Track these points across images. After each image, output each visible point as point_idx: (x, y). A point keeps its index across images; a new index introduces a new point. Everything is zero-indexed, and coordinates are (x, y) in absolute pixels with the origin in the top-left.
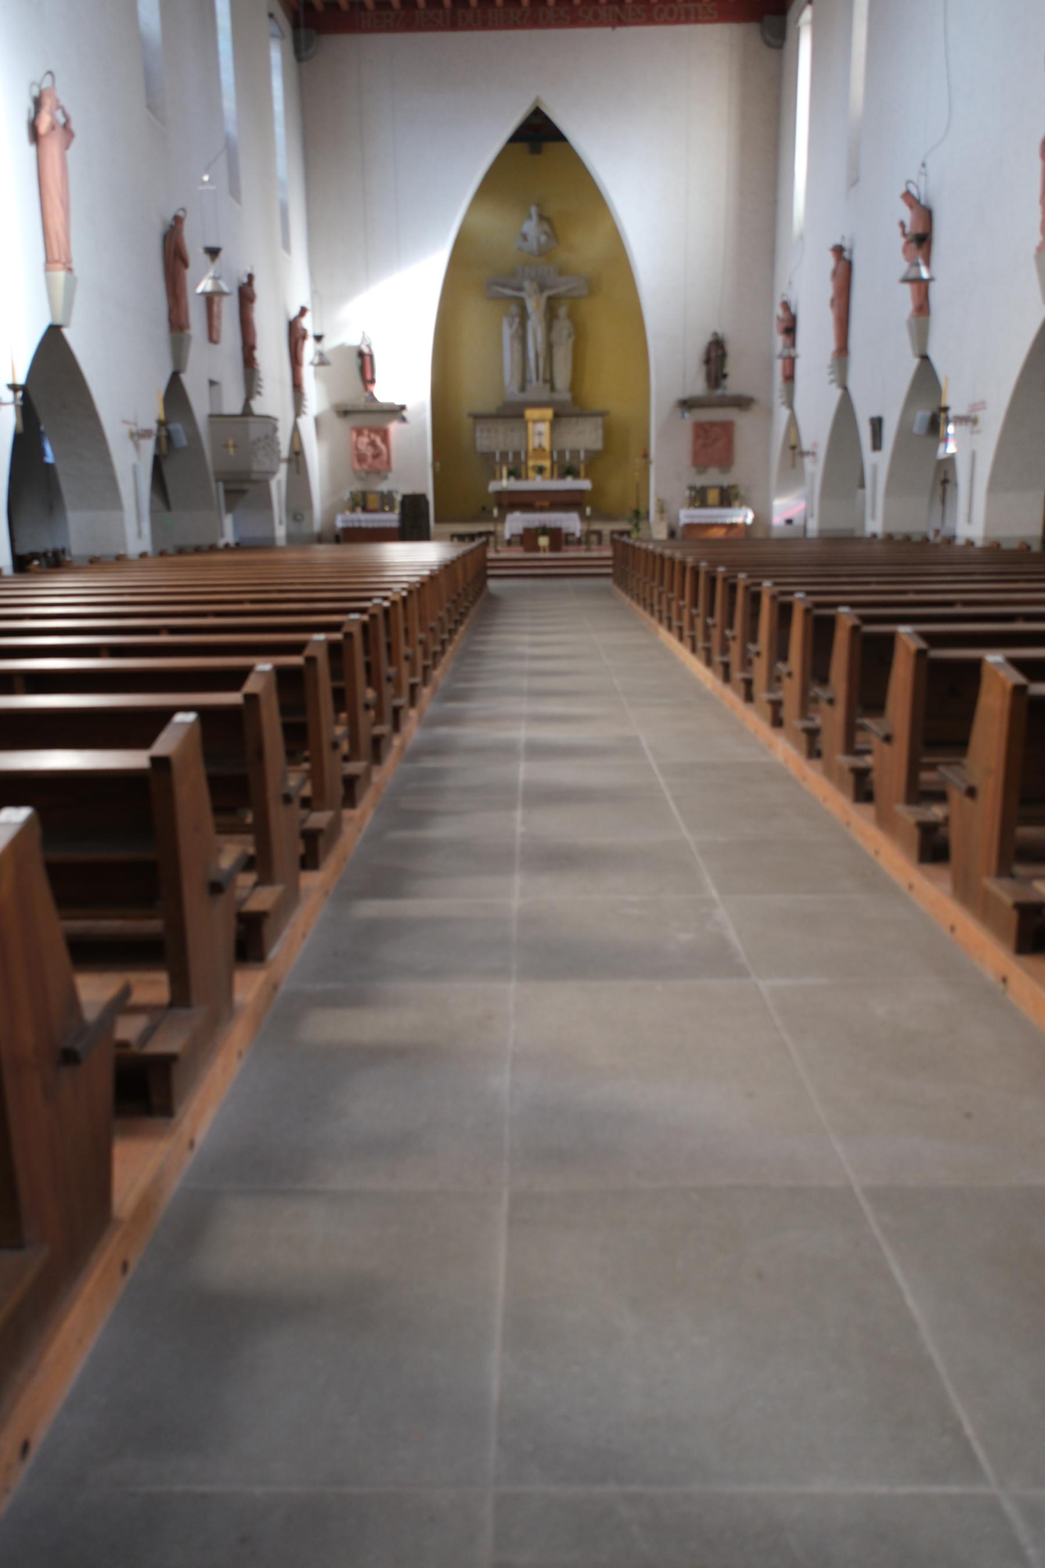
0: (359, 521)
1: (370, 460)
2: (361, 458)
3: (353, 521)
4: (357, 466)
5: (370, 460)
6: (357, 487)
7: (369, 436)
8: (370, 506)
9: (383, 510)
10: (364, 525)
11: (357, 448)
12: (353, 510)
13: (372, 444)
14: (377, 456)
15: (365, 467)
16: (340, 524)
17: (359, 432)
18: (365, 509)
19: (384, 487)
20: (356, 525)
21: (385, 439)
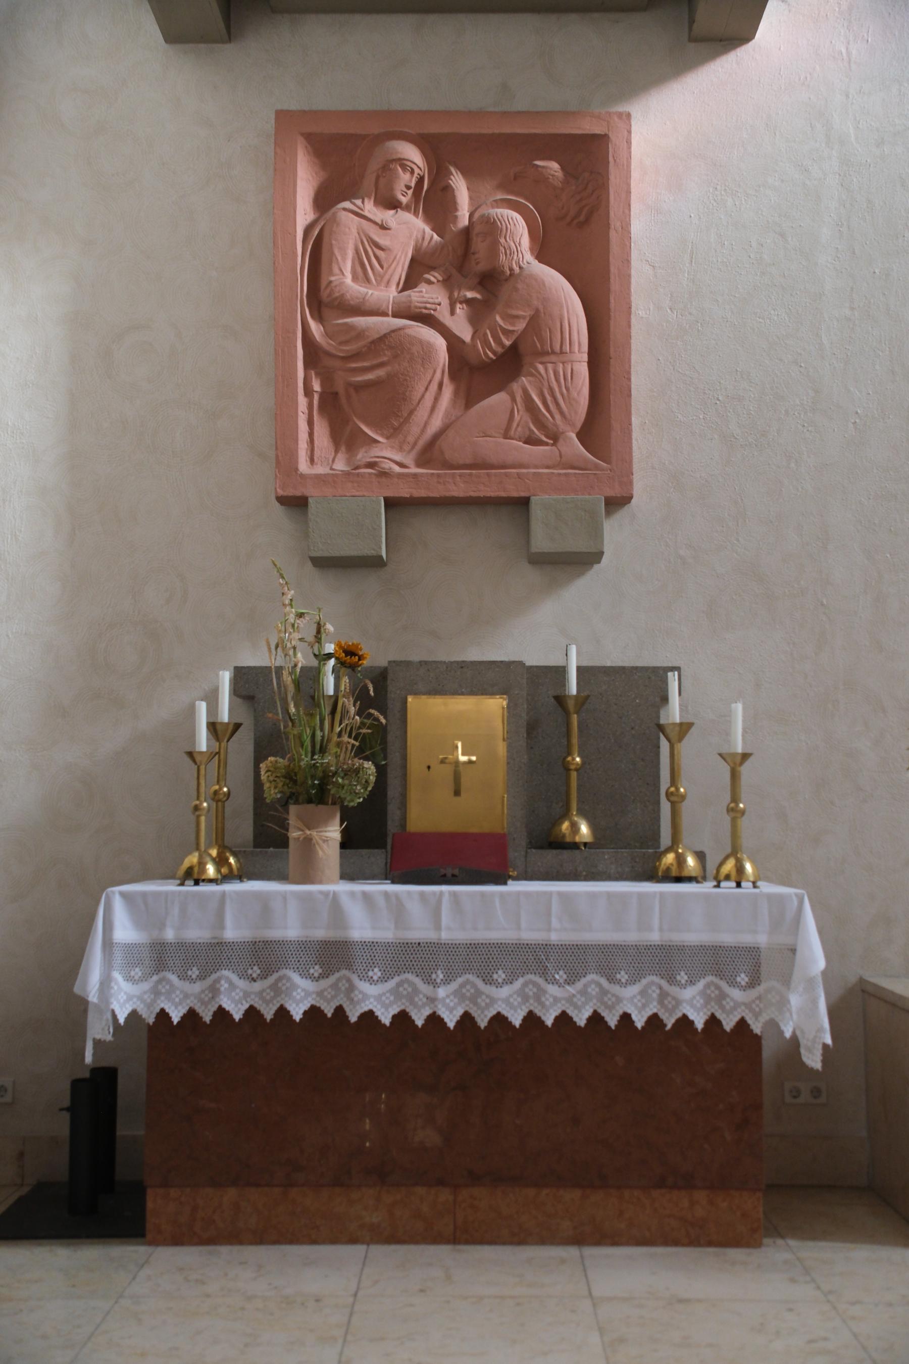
0: (333, 956)
1: (434, 403)
2: (351, 384)
3: (264, 957)
4: (316, 455)
5: (434, 403)
6: (299, 628)
7: (434, 201)
8: (427, 810)
9: (546, 849)
10: (375, 997)
11: (320, 300)
12: (266, 845)
13: (468, 264)
14: (482, 372)
15: (389, 454)
16: (117, 992)
17: (346, 159)
18: (381, 841)
19: (560, 633)
20: (301, 996)
21: (581, 228)
